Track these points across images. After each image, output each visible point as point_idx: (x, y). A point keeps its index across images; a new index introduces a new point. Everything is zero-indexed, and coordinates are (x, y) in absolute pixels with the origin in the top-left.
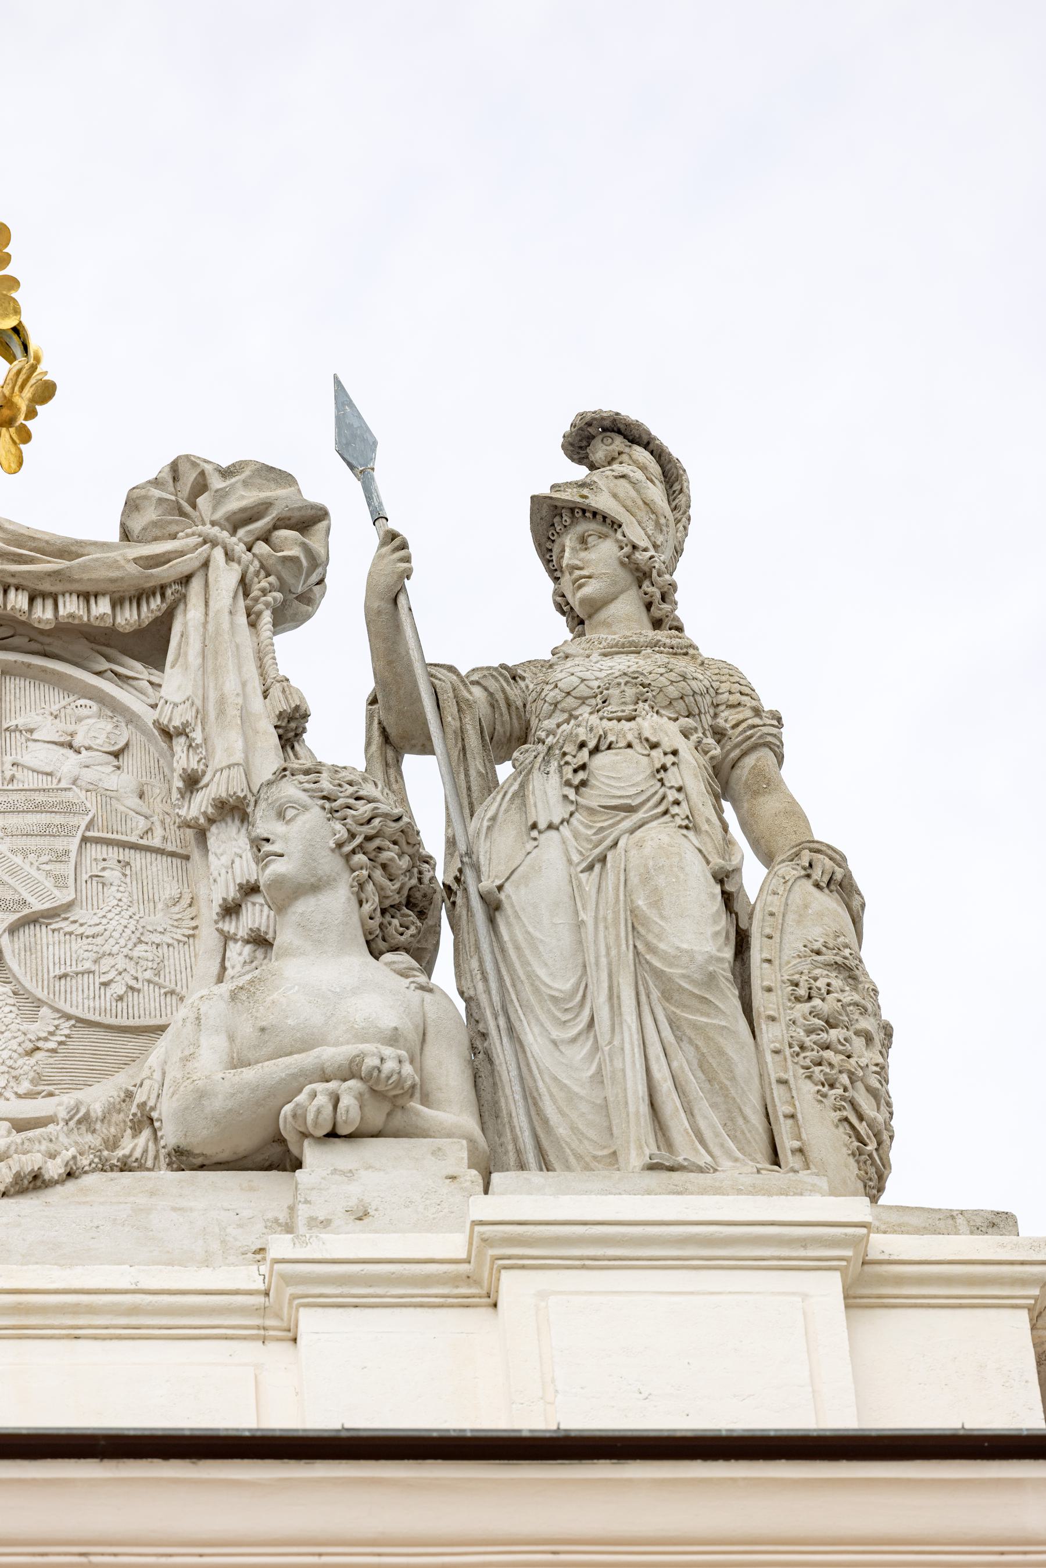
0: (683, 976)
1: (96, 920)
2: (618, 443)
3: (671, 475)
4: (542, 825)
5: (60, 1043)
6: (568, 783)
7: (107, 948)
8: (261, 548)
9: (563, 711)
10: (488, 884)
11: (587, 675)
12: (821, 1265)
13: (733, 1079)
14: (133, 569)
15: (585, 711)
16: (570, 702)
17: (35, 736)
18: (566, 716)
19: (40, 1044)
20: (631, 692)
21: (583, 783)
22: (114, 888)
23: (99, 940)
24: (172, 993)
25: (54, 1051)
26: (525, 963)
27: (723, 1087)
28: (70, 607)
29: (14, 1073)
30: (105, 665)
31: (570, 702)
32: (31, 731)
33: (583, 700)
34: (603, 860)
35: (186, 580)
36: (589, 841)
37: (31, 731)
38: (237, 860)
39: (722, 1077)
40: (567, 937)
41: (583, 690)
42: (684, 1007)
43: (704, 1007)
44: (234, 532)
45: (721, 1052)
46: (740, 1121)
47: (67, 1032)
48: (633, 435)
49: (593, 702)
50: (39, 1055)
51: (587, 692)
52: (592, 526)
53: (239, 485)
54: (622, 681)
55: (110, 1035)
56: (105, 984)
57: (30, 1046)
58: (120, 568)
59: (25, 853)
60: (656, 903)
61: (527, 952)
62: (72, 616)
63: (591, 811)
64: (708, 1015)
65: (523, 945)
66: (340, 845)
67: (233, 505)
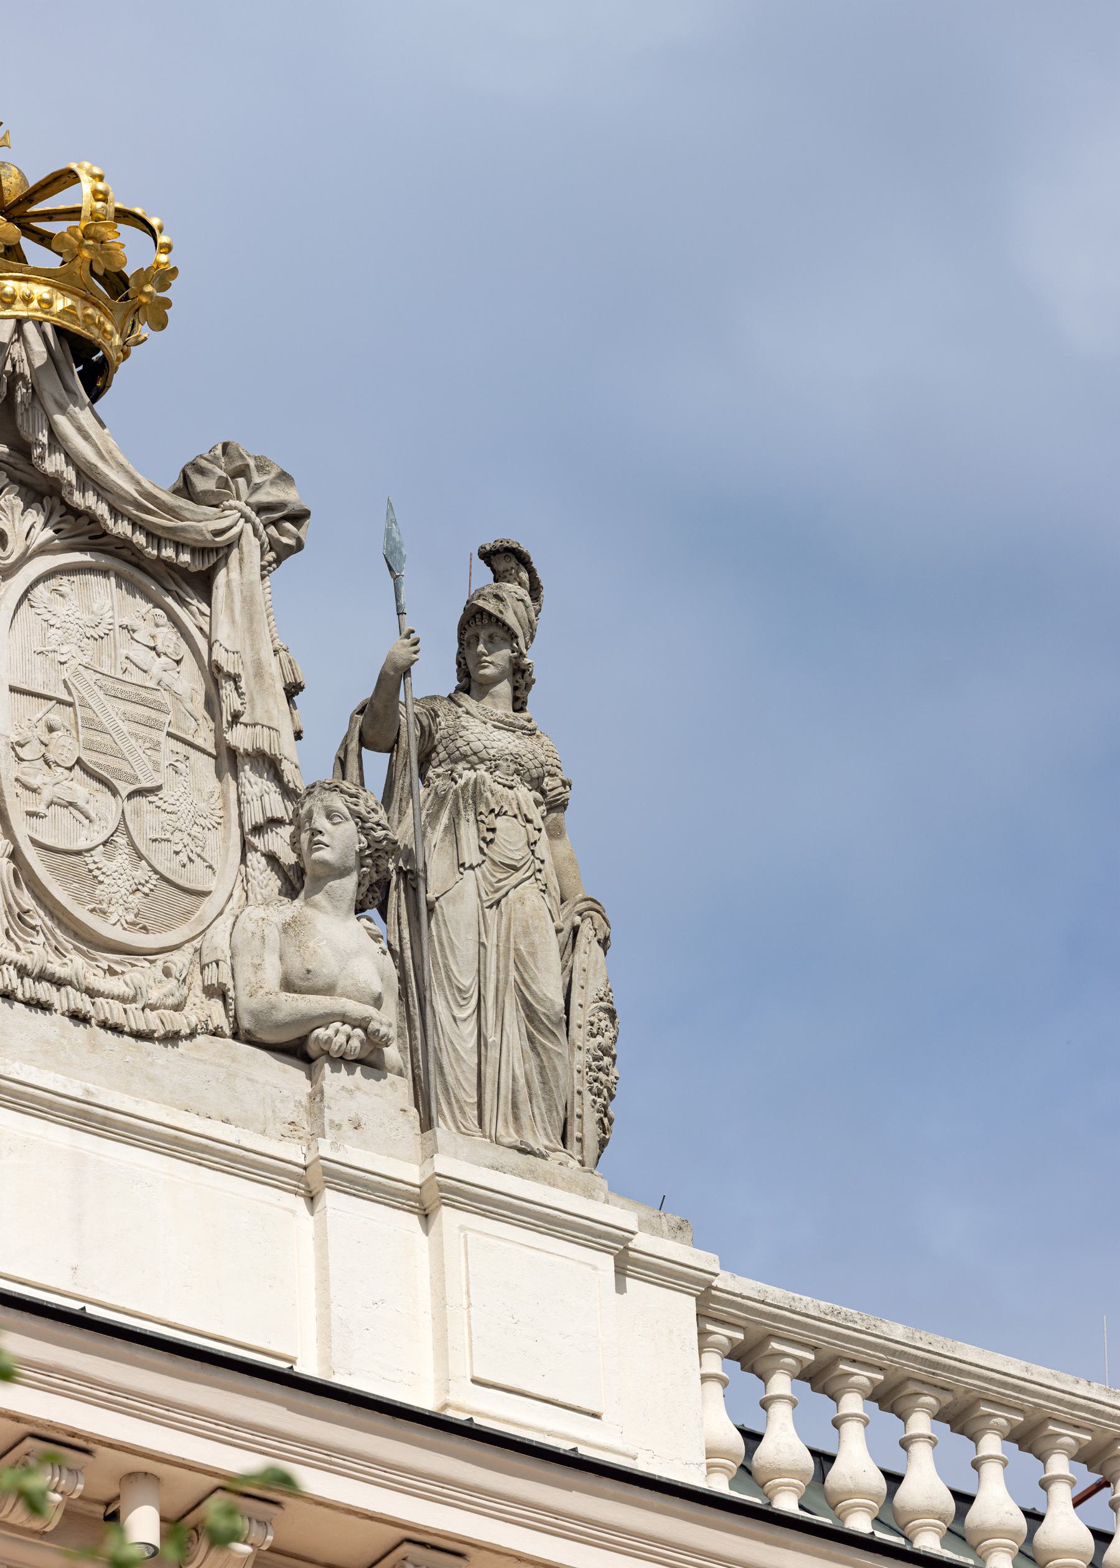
0: (544, 1014)
1: (172, 801)
2: (513, 563)
3: (535, 589)
4: (467, 865)
5: (152, 890)
6: (484, 839)
7: (178, 825)
8: (272, 530)
9: (468, 762)
10: (431, 896)
11: (487, 743)
12: (605, 1249)
13: (557, 1087)
14: (209, 536)
15: (482, 767)
16: (474, 758)
17: (135, 636)
18: (469, 766)
19: (140, 887)
20: (513, 767)
21: (492, 841)
22: (182, 778)
23: (173, 817)
24: (210, 867)
25: (147, 895)
26: (445, 957)
27: (551, 1090)
28: (168, 552)
29: (127, 905)
30: (174, 587)
31: (474, 758)
32: (134, 631)
33: (482, 761)
34: (498, 902)
35: (230, 546)
36: (493, 886)
37: (134, 631)
38: (266, 796)
39: (552, 1084)
40: (473, 948)
41: (484, 754)
42: (540, 1032)
43: (551, 1037)
44: (258, 514)
45: (555, 1069)
46: (555, 1114)
47: (154, 882)
48: (522, 559)
49: (488, 763)
50: (139, 894)
51: (486, 756)
52: (501, 633)
53: (268, 483)
54: (510, 758)
55: (177, 891)
56: (177, 853)
57: (134, 887)
58: (203, 535)
59: (136, 736)
60: (533, 954)
61: (448, 950)
62: (169, 557)
63: (494, 862)
64: (552, 1043)
65: (446, 944)
66: (361, 850)
67: (262, 497)
